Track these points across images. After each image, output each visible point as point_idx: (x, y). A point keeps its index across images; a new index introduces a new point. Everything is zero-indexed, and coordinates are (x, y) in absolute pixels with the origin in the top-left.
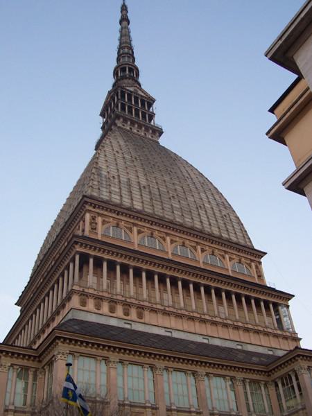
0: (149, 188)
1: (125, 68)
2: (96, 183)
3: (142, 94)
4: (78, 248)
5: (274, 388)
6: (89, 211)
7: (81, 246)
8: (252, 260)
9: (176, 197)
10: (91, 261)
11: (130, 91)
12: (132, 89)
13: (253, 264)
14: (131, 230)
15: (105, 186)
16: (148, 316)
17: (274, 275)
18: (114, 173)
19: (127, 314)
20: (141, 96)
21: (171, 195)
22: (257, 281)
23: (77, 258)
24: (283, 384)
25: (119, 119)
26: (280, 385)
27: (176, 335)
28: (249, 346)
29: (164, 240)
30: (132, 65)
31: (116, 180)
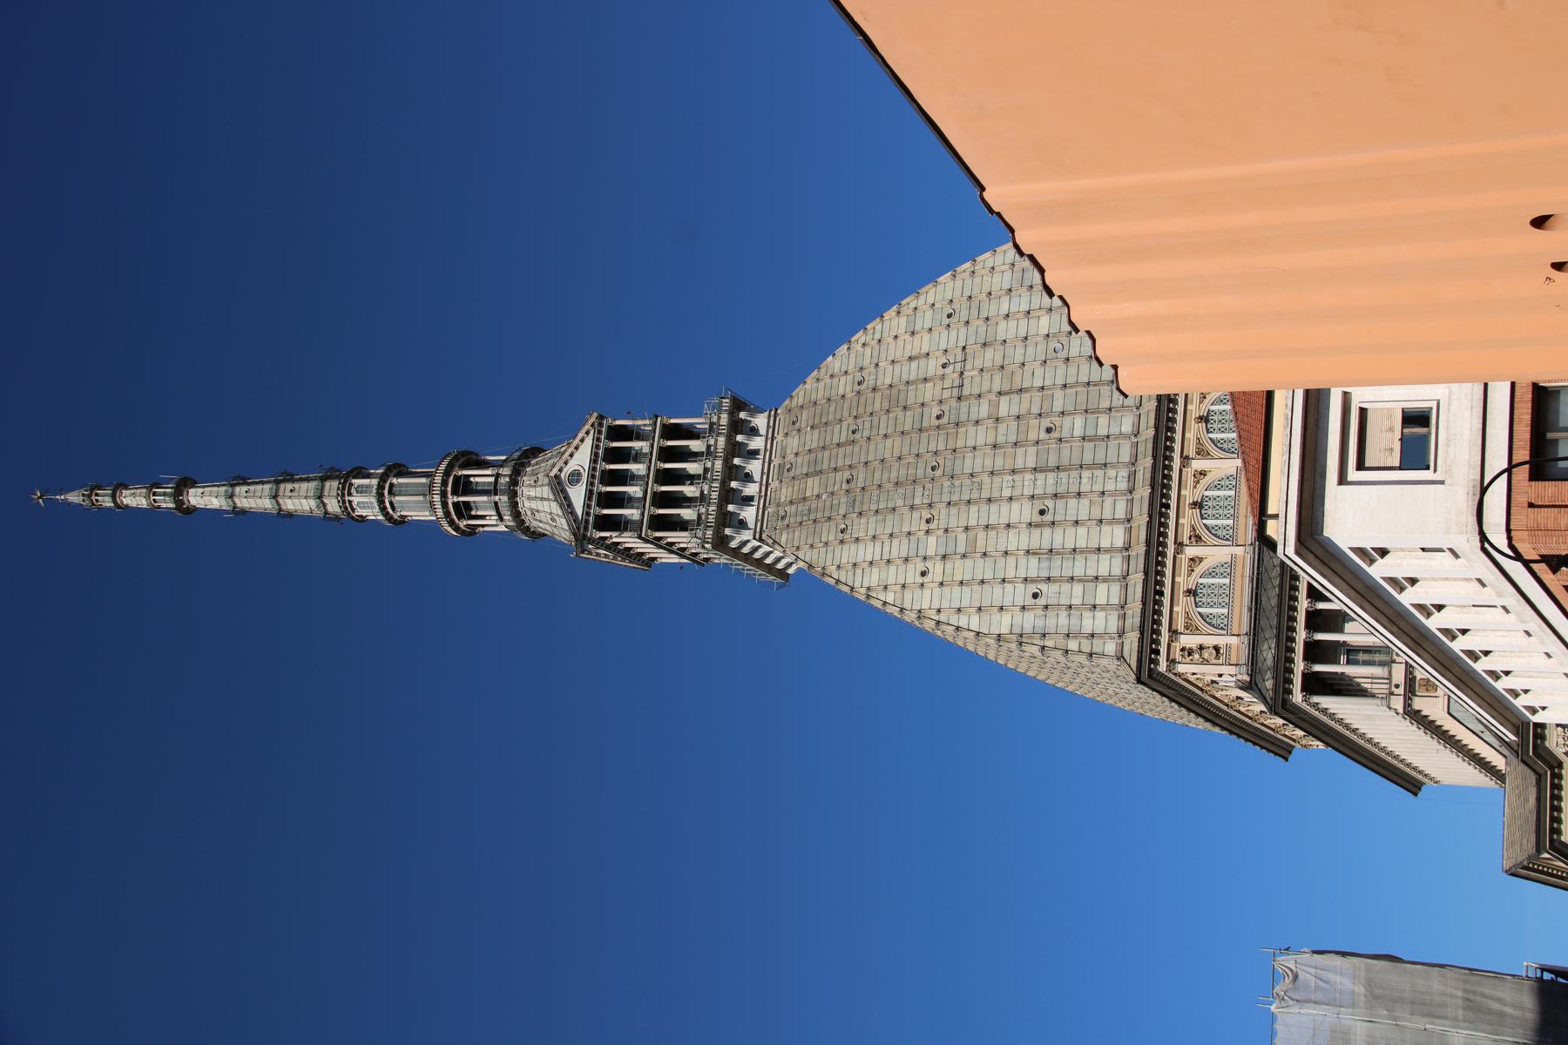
0: (1043, 497)
1: (456, 505)
2: (1073, 645)
4: (1297, 697)
6: (1172, 662)
7: (1290, 692)
9: (1046, 423)
10: (1318, 668)
11: (589, 494)
12: (577, 495)
14: (1194, 561)
15: (1074, 621)
18: (1022, 594)
20: (595, 461)
21: (1043, 435)
23: (1315, 699)
25: (726, 540)
29: (1203, 473)
30: (444, 483)
31: (1044, 587)
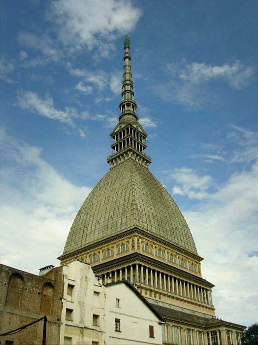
1: (130, 104)
3: (141, 131)
4: (137, 262)
5: (207, 335)
6: (137, 236)
8: (197, 263)
13: (197, 265)
16: (163, 299)
17: (207, 273)
19: (155, 297)
20: (141, 132)
22: (197, 275)
24: (212, 335)
26: (210, 335)
27: (172, 308)
28: (197, 313)
31: (144, 213)
